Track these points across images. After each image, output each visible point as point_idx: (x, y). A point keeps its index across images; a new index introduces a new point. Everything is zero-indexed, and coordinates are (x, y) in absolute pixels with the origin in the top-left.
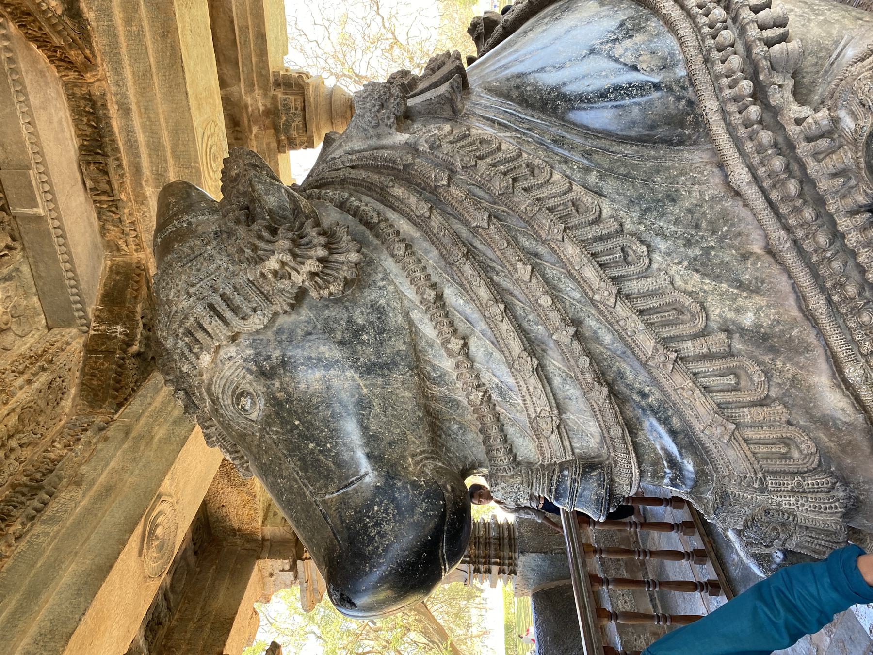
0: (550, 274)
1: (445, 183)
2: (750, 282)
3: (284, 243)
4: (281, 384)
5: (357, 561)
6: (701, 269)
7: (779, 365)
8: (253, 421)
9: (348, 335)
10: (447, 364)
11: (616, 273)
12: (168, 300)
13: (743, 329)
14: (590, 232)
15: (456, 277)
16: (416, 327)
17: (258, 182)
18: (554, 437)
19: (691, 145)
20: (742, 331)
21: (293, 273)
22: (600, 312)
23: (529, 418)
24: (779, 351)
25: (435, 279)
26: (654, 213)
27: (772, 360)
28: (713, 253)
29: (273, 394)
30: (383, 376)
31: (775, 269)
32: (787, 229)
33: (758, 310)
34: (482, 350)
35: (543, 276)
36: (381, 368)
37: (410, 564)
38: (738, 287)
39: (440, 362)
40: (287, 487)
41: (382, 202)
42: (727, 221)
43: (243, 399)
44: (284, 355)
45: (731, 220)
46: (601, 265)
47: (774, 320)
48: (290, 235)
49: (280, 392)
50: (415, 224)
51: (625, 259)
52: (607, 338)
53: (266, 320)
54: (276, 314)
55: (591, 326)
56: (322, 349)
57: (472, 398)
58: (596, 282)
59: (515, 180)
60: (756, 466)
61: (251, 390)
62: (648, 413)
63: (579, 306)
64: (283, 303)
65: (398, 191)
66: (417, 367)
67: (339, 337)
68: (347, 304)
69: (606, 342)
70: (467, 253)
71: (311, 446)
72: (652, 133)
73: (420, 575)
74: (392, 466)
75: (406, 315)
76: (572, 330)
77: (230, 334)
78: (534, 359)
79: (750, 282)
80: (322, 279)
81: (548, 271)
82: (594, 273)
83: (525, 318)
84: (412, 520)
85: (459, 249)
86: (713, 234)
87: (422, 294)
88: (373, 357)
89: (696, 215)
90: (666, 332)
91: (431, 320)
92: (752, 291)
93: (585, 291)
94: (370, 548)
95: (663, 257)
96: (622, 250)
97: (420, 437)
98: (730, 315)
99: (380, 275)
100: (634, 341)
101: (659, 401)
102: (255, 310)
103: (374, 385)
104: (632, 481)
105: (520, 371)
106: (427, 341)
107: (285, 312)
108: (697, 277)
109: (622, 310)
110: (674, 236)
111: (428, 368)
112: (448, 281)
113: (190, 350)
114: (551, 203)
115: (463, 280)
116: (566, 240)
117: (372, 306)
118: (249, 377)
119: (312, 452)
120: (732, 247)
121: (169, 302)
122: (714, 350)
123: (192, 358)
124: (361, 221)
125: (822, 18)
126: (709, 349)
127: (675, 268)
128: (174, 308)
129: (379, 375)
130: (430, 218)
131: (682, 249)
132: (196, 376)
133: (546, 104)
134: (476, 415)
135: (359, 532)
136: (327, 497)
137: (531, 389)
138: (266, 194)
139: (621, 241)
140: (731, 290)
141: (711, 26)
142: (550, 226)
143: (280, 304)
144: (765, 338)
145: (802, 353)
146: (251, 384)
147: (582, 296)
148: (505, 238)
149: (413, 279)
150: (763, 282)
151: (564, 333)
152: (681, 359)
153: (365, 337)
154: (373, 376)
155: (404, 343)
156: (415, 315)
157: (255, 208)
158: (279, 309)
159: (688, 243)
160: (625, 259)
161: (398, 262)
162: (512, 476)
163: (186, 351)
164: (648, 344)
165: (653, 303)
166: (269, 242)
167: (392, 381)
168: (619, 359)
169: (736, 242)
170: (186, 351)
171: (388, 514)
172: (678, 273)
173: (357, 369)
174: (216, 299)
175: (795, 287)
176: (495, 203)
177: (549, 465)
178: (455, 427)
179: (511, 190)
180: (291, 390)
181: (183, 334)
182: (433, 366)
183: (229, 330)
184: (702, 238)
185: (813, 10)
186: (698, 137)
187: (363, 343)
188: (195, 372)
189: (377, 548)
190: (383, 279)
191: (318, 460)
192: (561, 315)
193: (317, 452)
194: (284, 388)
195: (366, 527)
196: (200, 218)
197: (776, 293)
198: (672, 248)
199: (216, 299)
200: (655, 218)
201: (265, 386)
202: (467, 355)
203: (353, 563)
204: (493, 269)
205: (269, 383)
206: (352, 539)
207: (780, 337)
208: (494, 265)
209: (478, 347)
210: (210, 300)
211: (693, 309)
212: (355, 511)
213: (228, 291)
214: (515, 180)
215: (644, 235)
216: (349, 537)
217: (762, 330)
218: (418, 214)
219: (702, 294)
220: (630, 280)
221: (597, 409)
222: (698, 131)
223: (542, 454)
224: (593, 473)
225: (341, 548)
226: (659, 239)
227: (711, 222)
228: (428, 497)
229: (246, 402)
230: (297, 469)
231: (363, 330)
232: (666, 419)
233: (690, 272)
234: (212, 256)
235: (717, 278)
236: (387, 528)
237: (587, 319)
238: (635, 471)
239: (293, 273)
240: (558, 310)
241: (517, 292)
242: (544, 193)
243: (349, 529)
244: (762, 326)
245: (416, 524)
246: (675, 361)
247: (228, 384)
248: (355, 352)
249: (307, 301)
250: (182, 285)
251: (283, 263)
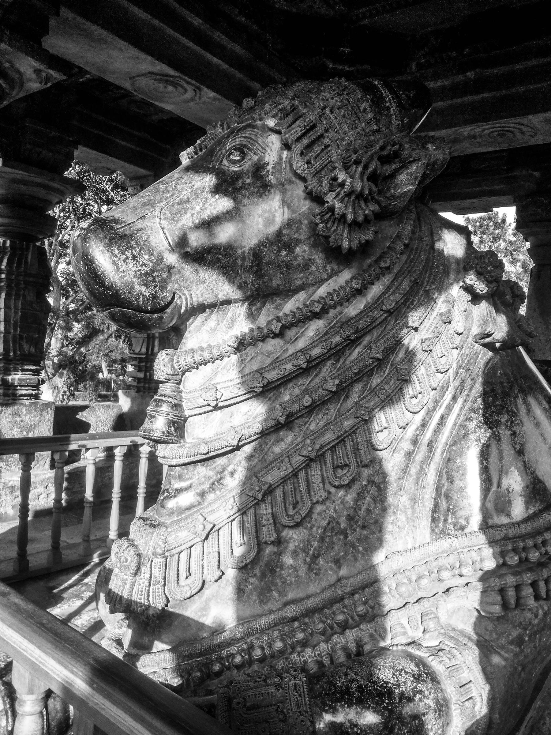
0: (330, 407)
2: (317, 565)
3: (358, 186)
4: (249, 184)
5: (107, 241)
6: (330, 527)
7: (252, 580)
8: (221, 162)
9: (286, 239)
12: (321, 91)
13: (280, 554)
15: (332, 330)
16: (292, 296)
17: (417, 167)
19: (431, 527)
20: (279, 554)
21: (334, 194)
23: (217, 384)
24: (262, 581)
25: (332, 313)
26: (376, 494)
27: (255, 575)
28: (342, 537)
29: (241, 177)
30: (251, 267)
31: (324, 584)
32: (352, 594)
33: (295, 568)
34: (272, 349)
35: (329, 400)
36: (258, 265)
37: (103, 281)
38: (313, 554)
39: (264, 315)
40: (169, 189)
41: (400, 271)
42: (366, 551)
43: (238, 153)
44: (271, 186)
45: (367, 554)
47: (286, 579)
48: (366, 192)
49: (242, 183)
51: (338, 467)
52: (277, 449)
53: (299, 172)
54: (304, 180)
55: (287, 436)
58: (322, 441)
60: (174, 551)
61: (245, 160)
62: (219, 476)
63: (304, 428)
64: (312, 186)
65: (405, 285)
66: (258, 294)
67: (284, 232)
69: (274, 447)
70: (350, 340)
71: (198, 208)
72: (442, 497)
73: (97, 289)
74: (179, 271)
76: (282, 420)
77: (290, 142)
78: (261, 389)
79: (317, 565)
80: (330, 217)
81: (333, 405)
82: (328, 441)
83: (296, 385)
84: (136, 284)
85: (353, 333)
86: (357, 539)
87: (319, 302)
88: (267, 259)
89: (373, 527)
91: (298, 308)
92: (310, 565)
93: (315, 433)
94: (116, 251)
95: (340, 498)
96: (347, 465)
97: (202, 295)
98: (291, 546)
99: (336, 267)
101: (227, 486)
102: (308, 162)
103: (244, 259)
104: (167, 458)
105: (253, 377)
106: (280, 304)
107: (306, 187)
108: (324, 523)
110: (357, 507)
112: (329, 324)
113: (280, 110)
115: (329, 336)
116: (356, 420)
117: (310, 259)
119: (192, 208)
120: (346, 554)
121: (319, 92)
123: (274, 112)
124: (384, 253)
125: (527, 639)
126: (264, 525)
127: (332, 506)
128: (314, 96)
129: (252, 263)
130: (382, 310)
131: (346, 513)
132: (260, 115)
133: (475, 413)
134: (221, 342)
135: (129, 243)
136: (158, 220)
138: (408, 173)
139: (353, 465)
140: (312, 549)
141: (524, 549)
142: (368, 408)
143: (312, 183)
144: (273, 571)
145: (259, 597)
146: (250, 159)
147: (311, 431)
148: (360, 371)
149: (331, 295)
150: (316, 574)
151: (281, 414)
152: (257, 504)
153: (284, 253)
154: (251, 258)
155: (278, 285)
156: (302, 296)
157: (395, 163)
158: (308, 183)
159: (350, 518)
160: (338, 467)
161: (347, 282)
162: (173, 367)
163: (280, 107)
165: (303, 486)
166: (362, 174)
167: (247, 274)
168: (261, 457)
169: (350, 557)
170: (280, 107)
171: (141, 266)
172: (327, 508)
174: (319, 131)
175: (308, 597)
176: (392, 365)
177: (181, 397)
179: (400, 378)
180: (243, 192)
181: (294, 105)
182: (260, 309)
183: (292, 141)
184: (355, 530)
185: (535, 634)
186: (436, 533)
187: (279, 251)
188: (263, 115)
189: (116, 256)
190: (332, 269)
191: (186, 213)
192: (296, 413)
193: (193, 212)
194: (245, 187)
195: (131, 248)
196: (394, 117)
197: (308, 583)
198: (347, 505)
199: (319, 131)
200: (372, 494)
201: (248, 170)
202: (268, 336)
203: (105, 237)
204: (337, 361)
205: (250, 174)
206: (123, 237)
207: (272, 582)
208: (341, 362)
210: (319, 126)
211: (296, 517)
212: (145, 241)
213: (326, 141)
215: (359, 483)
216: (125, 235)
217: (278, 570)
218: (385, 301)
219: (309, 525)
220: (321, 470)
221: (221, 436)
222: (441, 534)
223: (190, 392)
224: (173, 429)
225: (118, 229)
226: (354, 495)
227: (366, 537)
228: (154, 297)
229: (236, 157)
230: (181, 197)
231: (289, 251)
232: (213, 489)
233: (328, 518)
234: (356, 128)
235: (322, 539)
236: (131, 263)
237: (293, 434)
239: (334, 194)
240: (300, 411)
241: (317, 380)
243: (131, 235)
244: (282, 569)
245: (131, 287)
246: (255, 499)
247: (251, 141)
248: (272, 244)
249: (314, 205)
250: (332, 102)
251: (342, 185)
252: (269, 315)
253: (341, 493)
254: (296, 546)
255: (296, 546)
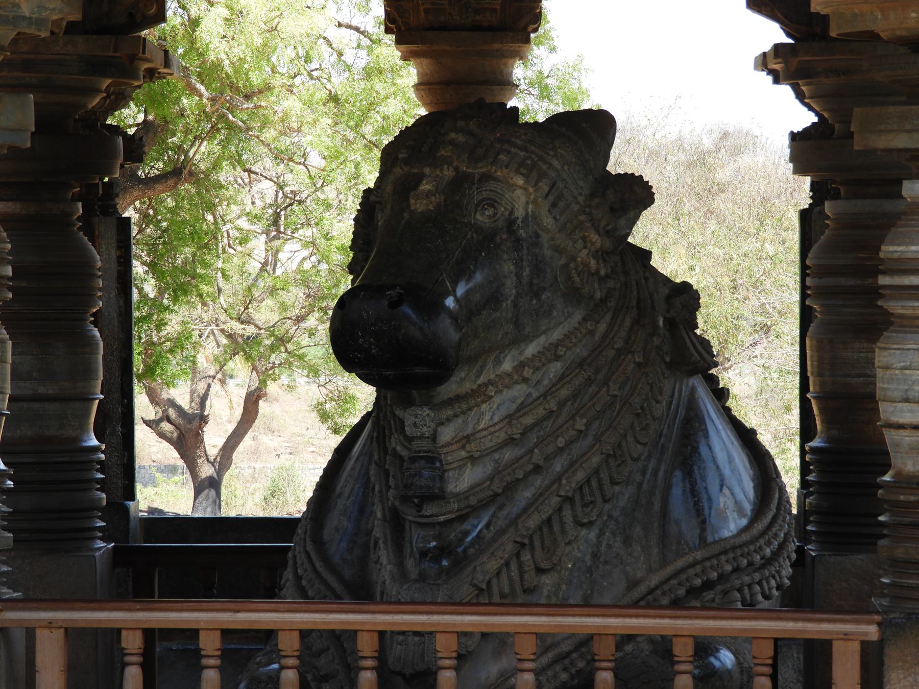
1: (637, 360)
10: (507, 366)
11: (577, 498)
14: (604, 475)
18: (463, 453)
22: (549, 487)
28: (588, 575)
46: (581, 486)
50: (605, 336)
53: (549, 227)
56: (527, 269)
57: (490, 387)
59: (638, 415)
61: (498, 215)
68: (554, 286)
75: (544, 332)
90: (536, 539)
96: (592, 502)
100: (533, 513)
109: (555, 500)
110: (599, 544)
111: (506, 352)
114: (624, 444)
117: (552, 305)
118: (507, 213)
122: (526, 576)
130: (613, 348)
131: (590, 551)
137: (497, 434)
139: (599, 500)
156: (542, 339)
164: (532, 523)
173: (516, 297)
178: (463, 375)
182: (506, 356)
184: (598, 567)
187: (531, 300)
208: (578, 401)
209: (519, 391)
214: (638, 415)
226: (597, 531)
238: (442, 518)
242: (630, 439)
252: (513, 362)
253: (584, 532)
254: (549, 591)
255: (549, 591)
